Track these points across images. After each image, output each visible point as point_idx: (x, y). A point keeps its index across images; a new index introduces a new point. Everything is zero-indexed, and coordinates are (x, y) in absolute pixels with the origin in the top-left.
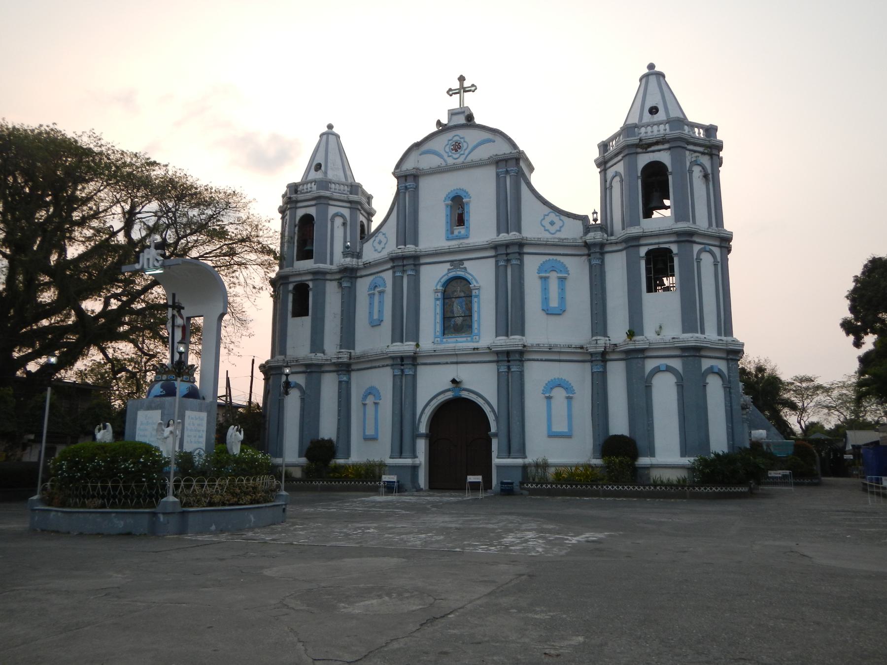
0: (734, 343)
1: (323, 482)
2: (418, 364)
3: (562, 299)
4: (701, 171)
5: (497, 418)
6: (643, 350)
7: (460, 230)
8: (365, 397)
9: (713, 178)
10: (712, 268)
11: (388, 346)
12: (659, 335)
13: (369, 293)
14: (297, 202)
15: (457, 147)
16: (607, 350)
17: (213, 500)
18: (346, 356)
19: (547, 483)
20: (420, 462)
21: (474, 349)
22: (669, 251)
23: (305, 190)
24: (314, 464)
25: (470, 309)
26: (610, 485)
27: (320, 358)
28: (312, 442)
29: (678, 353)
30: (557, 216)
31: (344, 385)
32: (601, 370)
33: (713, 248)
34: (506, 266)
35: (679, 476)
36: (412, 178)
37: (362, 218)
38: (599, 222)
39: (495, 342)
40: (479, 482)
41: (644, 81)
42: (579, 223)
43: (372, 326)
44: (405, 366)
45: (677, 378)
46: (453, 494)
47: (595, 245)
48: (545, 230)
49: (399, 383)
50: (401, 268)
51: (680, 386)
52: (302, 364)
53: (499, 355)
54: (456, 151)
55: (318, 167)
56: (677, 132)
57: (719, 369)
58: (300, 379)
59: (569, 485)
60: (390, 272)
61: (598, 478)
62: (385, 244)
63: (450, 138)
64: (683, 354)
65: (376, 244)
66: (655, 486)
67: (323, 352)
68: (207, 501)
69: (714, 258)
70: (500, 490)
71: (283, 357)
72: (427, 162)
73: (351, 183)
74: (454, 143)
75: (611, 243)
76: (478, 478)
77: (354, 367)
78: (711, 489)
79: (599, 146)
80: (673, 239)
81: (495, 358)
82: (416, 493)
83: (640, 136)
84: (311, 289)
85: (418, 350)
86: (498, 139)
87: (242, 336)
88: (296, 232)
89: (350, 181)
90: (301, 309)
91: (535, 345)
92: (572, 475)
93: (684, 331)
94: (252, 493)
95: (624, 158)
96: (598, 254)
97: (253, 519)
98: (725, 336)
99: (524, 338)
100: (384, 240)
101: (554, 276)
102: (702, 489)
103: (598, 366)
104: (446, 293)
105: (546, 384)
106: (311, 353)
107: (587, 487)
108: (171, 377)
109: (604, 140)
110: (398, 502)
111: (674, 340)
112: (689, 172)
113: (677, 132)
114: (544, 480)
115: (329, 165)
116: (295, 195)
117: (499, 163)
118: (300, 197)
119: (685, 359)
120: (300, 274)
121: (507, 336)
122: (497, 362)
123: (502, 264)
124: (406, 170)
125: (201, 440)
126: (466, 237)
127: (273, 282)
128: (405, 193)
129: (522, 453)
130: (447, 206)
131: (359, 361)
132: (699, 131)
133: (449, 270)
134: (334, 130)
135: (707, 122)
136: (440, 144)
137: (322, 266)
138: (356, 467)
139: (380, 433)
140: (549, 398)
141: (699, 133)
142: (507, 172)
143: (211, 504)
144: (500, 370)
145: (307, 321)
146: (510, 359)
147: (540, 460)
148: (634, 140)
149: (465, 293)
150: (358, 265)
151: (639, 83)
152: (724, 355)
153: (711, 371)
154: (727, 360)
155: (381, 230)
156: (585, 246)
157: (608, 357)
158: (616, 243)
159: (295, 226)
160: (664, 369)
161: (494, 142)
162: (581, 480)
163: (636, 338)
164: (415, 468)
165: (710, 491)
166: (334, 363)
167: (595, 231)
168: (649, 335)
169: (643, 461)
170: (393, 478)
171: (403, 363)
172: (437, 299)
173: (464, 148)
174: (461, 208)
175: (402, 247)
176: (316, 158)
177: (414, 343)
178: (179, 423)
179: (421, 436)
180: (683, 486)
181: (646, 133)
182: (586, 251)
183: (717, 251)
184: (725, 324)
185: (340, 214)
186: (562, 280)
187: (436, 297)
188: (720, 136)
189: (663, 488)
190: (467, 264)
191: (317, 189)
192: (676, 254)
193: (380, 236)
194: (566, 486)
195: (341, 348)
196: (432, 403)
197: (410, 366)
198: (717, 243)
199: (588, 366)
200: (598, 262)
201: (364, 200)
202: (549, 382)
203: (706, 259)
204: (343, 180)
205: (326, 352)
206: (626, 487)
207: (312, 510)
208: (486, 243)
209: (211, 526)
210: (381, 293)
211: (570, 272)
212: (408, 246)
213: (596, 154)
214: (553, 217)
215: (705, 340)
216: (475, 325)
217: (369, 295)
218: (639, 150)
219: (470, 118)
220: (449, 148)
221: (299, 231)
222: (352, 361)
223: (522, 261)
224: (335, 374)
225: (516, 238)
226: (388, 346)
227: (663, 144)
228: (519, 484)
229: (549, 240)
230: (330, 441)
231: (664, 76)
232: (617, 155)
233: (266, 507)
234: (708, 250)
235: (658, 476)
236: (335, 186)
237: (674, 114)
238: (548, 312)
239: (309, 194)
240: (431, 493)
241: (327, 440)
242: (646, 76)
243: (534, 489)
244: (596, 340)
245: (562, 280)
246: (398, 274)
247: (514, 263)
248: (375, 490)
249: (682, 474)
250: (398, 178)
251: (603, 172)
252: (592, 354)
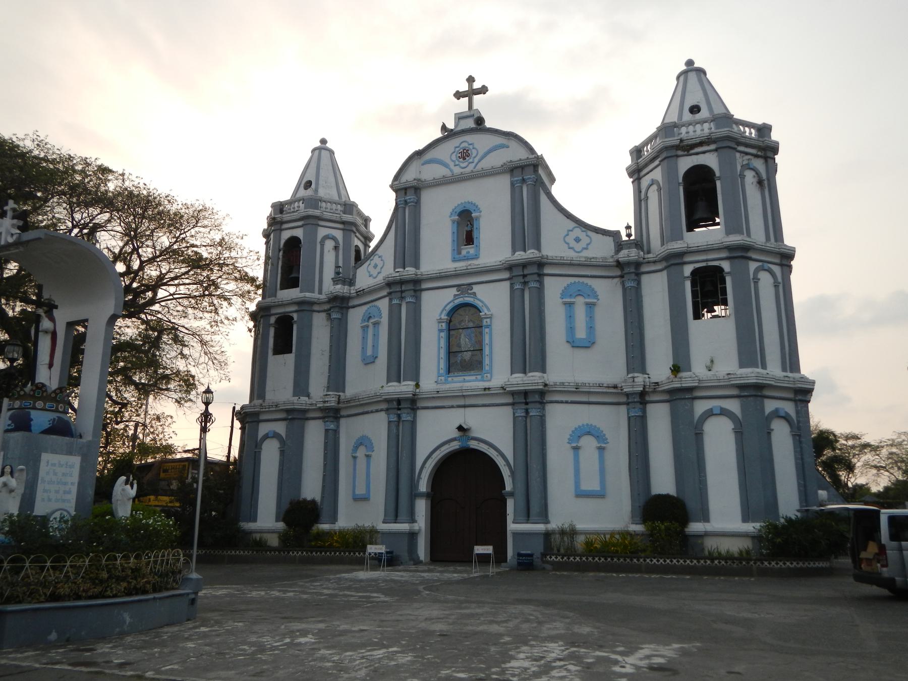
0: (803, 380)
1: (302, 553)
2: (418, 408)
3: (591, 329)
4: (754, 176)
5: (513, 474)
6: (691, 389)
7: (469, 250)
8: (356, 448)
9: (769, 185)
10: (772, 290)
11: (382, 387)
12: (710, 370)
13: (363, 325)
14: (282, 223)
15: (465, 155)
16: (647, 390)
17: (58, 591)
18: (334, 399)
19: (575, 555)
20: (420, 527)
21: (485, 389)
22: (720, 270)
23: (292, 210)
24: (292, 530)
25: (480, 342)
26: (654, 558)
27: (304, 402)
28: (291, 503)
29: (735, 392)
30: (583, 231)
31: (331, 433)
32: (640, 414)
33: (774, 267)
34: (523, 290)
35: (741, 548)
36: (413, 191)
37: (357, 242)
38: (633, 238)
39: (511, 380)
40: (489, 555)
41: (682, 78)
42: (609, 240)
43: (366, 364)
44: (402, 411)
45: (734, 422)
46: (459, 568)
47: (629, 264)
48: (570, 248)
49: (395, 431)
50: (399, 294)
51: (739, 433)
52: (282, 410)
53: (515, 396)
54: (464, 159)
55: (308, 184)
56: (726, 129)
57: (786, 413)
58: (280, 428)
59: (603, 557)
60: (387, 300)
61: (639, 548)
62: (382, 268)
63: (458, 145)
64: (743, 394)
65: (371, 268)
66: (712, 560)
67: (308, 396)
68: (48, 594)
69: (774, 279)
70: (516, 563)
71: (260, 401)
72: (430, 172)
73: (345, 202)
74: (462, 150)
75: (649, 262)
76: (488, 550)
77: (343, 413)
78: (785, 564)
79: (631, 152)
80: (724, 254)
81: (509, 400)
82: (413, 568)
83: (682, 136)
84: (295, 322)
85: (418, 390)
86: (513, 144)
87: (222, 381)
88: (281, 257)
89: (344, 200)
90: (283, 346)
91: (558, 384)
92: (605, 544)
93: (742, 365)
94: (132, 579)
95: (662, 163)
96: (633, 275)
97: (128, 620)
98: (791, 372)
99: (545, 375)
100: (380, 264)
101: (580, 301)
102: (773, 563)
103: (636, 409)
104: (451, 324)
105: (573, 432)
106: (293, 396)
107: (625, 560)
108: (26, 404)
109: (637, 145)
110: (385, 581)
111: (730, 376)
112: (740, 177)
113: (726, 129)
114: (571, 551)
115: (321, 182)
116: (280, 215)
117: (514, 171)
118: (286, 217)
119: (744, 399)
120: (282, 305)
121: (525, 372)
122: (513, 404)
123: (518, 287)
124: (405, 181)
125: (68, 497)
126: (476, 257)
127: (254, 316)
128: (404, 209)
129: (544, 516)
130: (453, 222)
131: (349, 405)
132: (750, 130)
133: (455, 295)
134: (327, 145)
135: (759, 121)
136: (446, 151)
137: (308, 295)
138: (342, 533)
139: (371, 494)
140: (576, 449)
141: (751, 133)
142: (524, 181)
143: (54, 597)
144: (517, 415)
145: (290, 358)
146: (527, 401)
147: (566, 526)
148: (673, 141)
149: (474, 322)
150: (350, 294)
151: (676, 82)
152: (791, 396)
153: (776, 414)
154: (795, 401)
155: (377, 253)
156: (617, 266)
157: (647, 398)
158: (655, 262)
159: (280, 250)
160: (718, 412)
161: (508, 147)
162: (617, 551)
163: (683, 374)
164: (412, 536)
165: (783, 566)
166: (320, 407)
167: (629, 248)
168: (698, 370)
169: (695, 527)
170: (381, 549)
171: (400, 407)
172: (441, 331)
173: (473, 155)
174: (469, 225)
175: (401, 270)
176: (307, 175)
177: (413, 383)
178: (22, 470)
179: (421, 495)
180: (748, 560)
181: (687, 133)
182: (618, 273)
183: (777, 270)
184: (791, 359)
185: (331, 237)
186: (590, 306)
187: (440, 328)
188: (774, 136)
189: (723, 562)
190: (476, 289)
191: (305, 208)
192: (728, 273)
193: (376, 260)
194: (600, 559)
195: (328, 391)
196: (434, 456)
197: (409, 410)
198: (777, 261)
199: (623, 408)
200: (633, 284)
201: (359, 221)
202: (576, 429)
203: (765, 279)
204: (336, 198)
205: (311, 395)
206: (675, 561)
207: (263, 593)
208: (499, 263)
209: (50, 633)
210: (376, 324)
211: (599, 297)
212: (407, 269)
213: (628, 161)
214: (578, 232)
215: (768, 376)
216: (487, 361)
217: (362, 327)
218: (680, 153)
219: (480, 121)
220: (456, 155)
221: (283, 256)
222: (340, 405)
223: (541, 283)
224: (321, 420)
225: (535, 256)
226: (382, 387)
227: (708, 145)
228: (539, 556)
229: (574, 259)
230: (313, 502)
231: (704, 73)
232: (653, 160)
233: (154, 599)
234: (766, 268)
235: (715, 546)
236: (326, 205)
237: (718, 110)
238: (574, 344)
239: (296, 214)
240: (432, 567)
241: (309, 501)
242: (684, 73)
243: (559, 562)
244: (633, 378)
245: (590, 306)
246: (395, 302)
247: (533, 285)
248: (360, 563)
249: (746, 544)
250: (396, 191)
251: (636, 181)
252: (627, 395)
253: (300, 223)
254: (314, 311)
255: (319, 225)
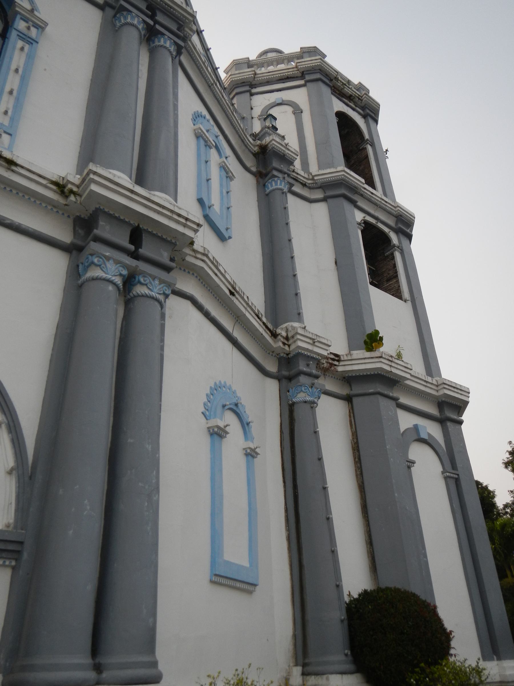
91: (210, 255)
144: (95, 272)
146: (143, 251)
156: (255, 155)
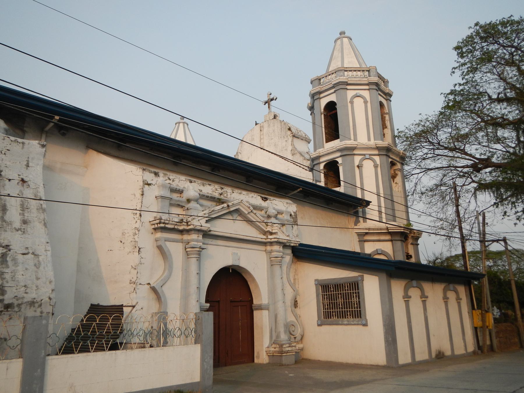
253: (333, 91)
254: (354, 155)
255: (347, 89)
